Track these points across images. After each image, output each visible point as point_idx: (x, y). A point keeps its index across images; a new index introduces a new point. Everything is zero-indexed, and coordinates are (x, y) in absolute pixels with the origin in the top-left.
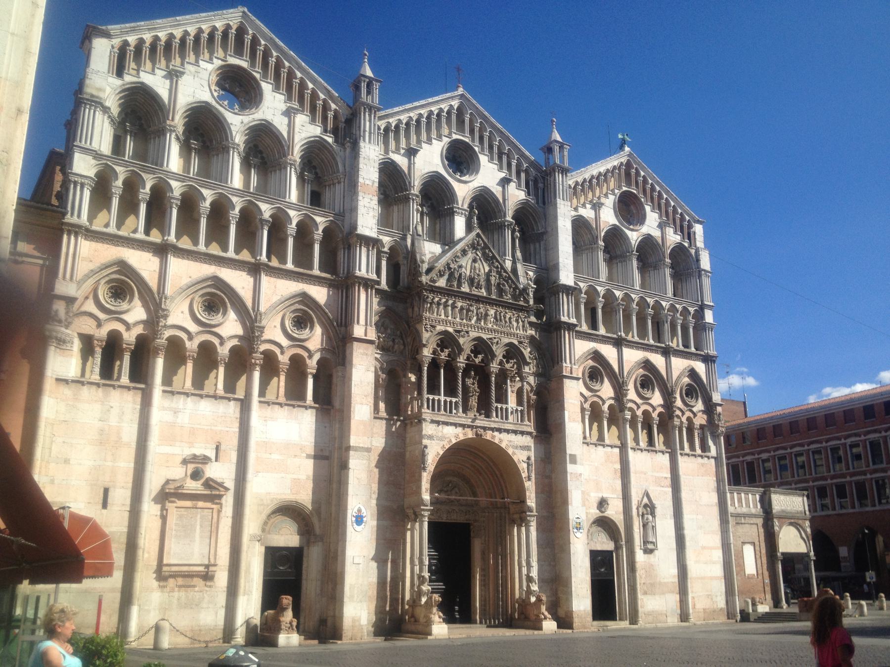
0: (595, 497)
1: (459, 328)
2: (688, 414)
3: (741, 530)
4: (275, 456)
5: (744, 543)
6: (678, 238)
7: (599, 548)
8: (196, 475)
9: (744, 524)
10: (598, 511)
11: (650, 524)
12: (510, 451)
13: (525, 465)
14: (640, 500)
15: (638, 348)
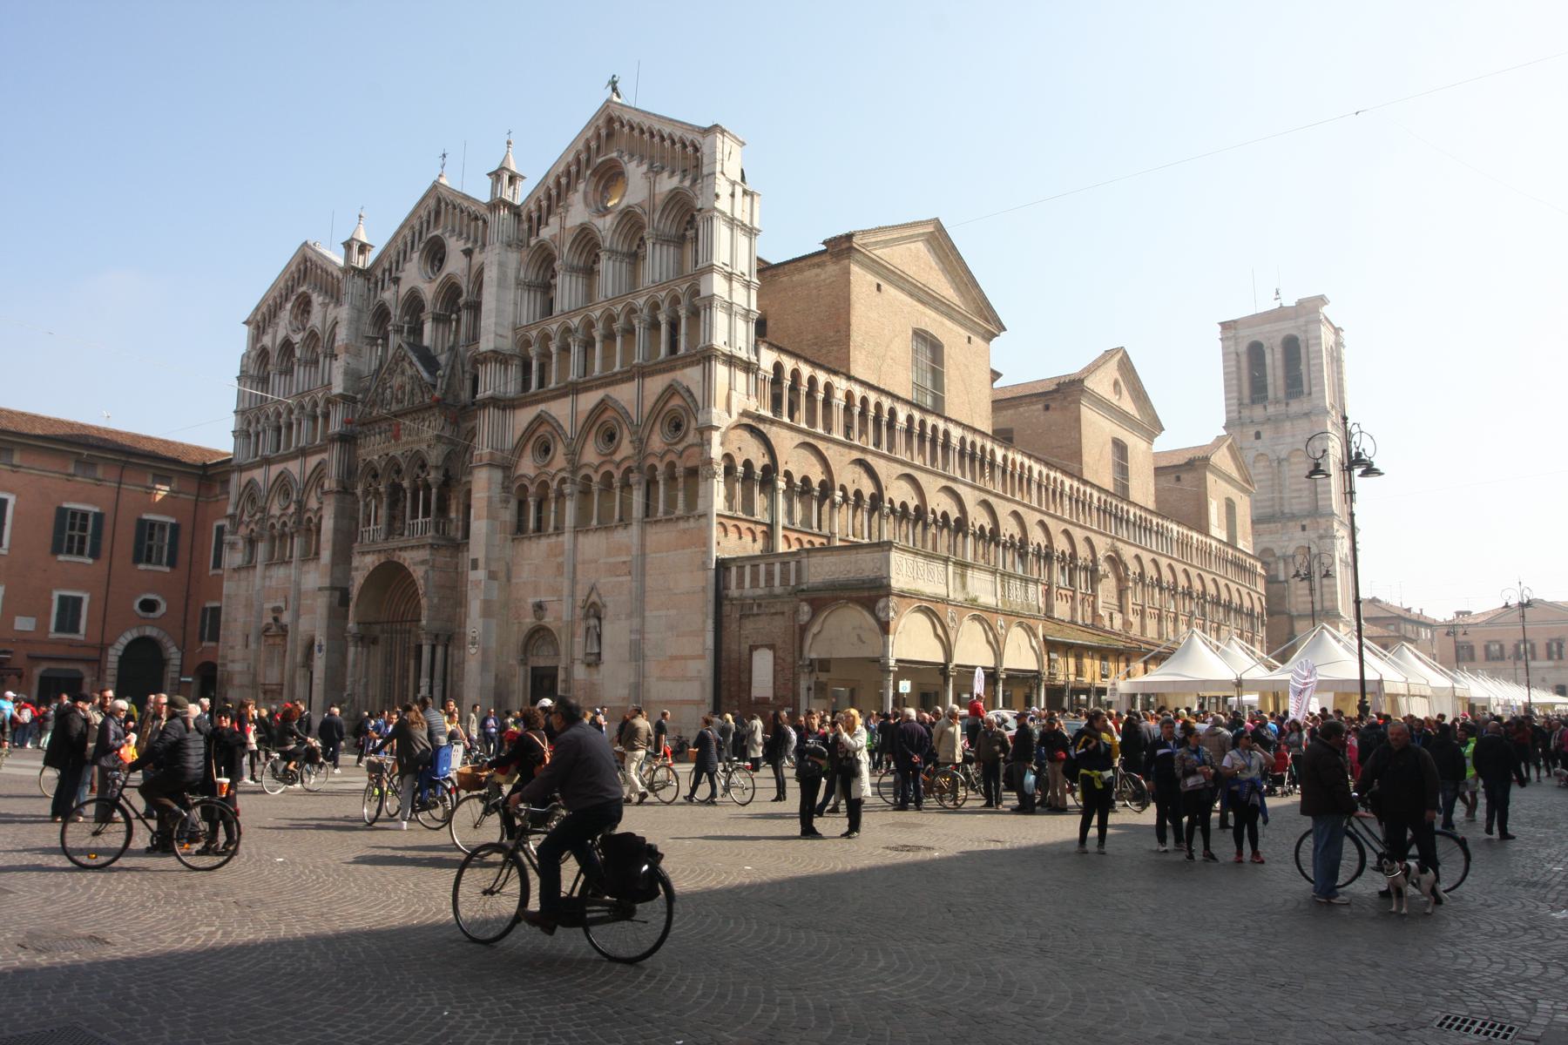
0: (531, 600)
1: (381, 453)
2: (668, 458)
3: (749, 626)
4: (309, 602)
5: (753, 648)
6: (674, 182)
7: (542, 663)
8: (276, 619)
9: (758, 615)
10: (534, 620)
11: (592, 630)
12: (411, 570)
13: (422, 581)
14: (585, 598)
15: (598, 387)
